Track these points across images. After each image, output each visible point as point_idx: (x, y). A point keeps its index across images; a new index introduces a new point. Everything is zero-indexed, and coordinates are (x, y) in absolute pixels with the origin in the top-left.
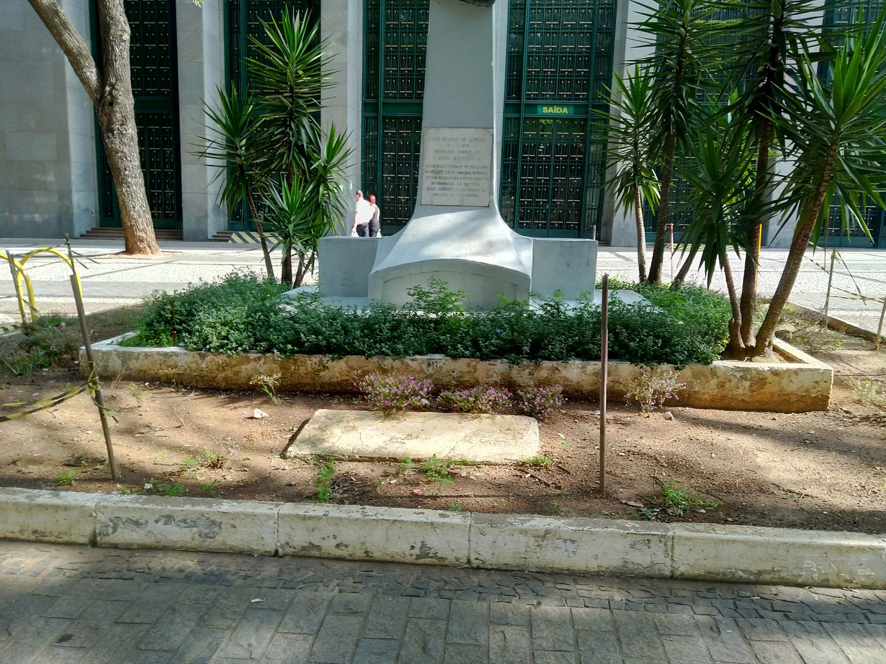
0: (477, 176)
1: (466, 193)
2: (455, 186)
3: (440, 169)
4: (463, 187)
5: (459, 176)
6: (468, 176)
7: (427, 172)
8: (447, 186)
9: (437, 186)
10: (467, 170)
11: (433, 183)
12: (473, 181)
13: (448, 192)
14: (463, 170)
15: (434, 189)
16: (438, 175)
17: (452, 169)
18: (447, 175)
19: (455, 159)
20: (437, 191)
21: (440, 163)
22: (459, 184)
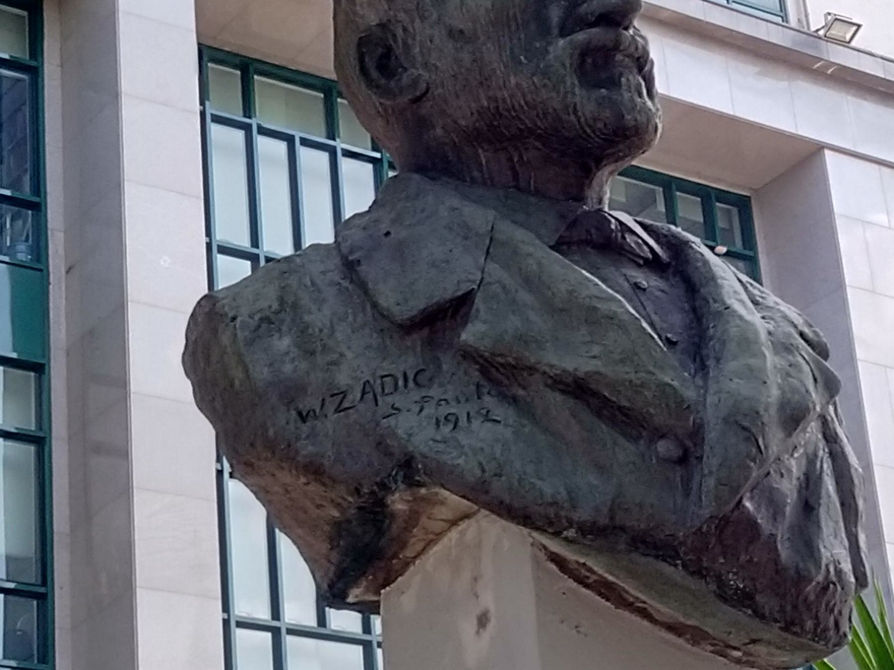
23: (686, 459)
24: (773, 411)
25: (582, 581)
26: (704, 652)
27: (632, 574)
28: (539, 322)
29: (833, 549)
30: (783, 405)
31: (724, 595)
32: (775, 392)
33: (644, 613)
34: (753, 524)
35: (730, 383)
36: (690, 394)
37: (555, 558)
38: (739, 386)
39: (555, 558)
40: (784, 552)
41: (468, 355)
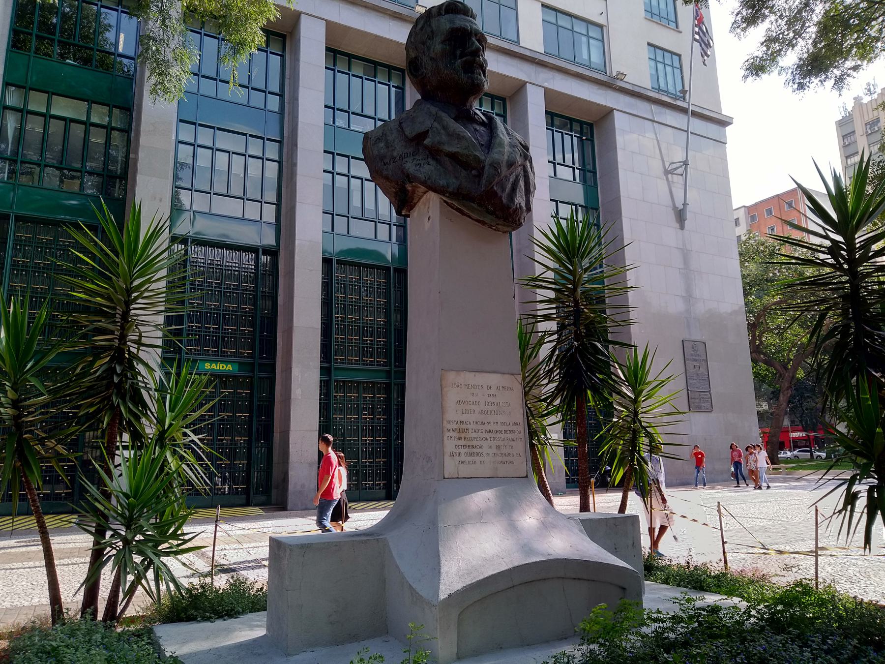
0: (509, 435)
1: (499, 459)
2: (485, 450)
3: (464, 426)
4: (495, 450)
5: (488, 435)
6: (498, 435)
7: (448, 430)
8: (475, 450)
9: (462, 451)
10: (498, 427)
11: (457, 447)
12: (506, 443)
13: (477, 459)
14: (493, 427)
15: (459, 454)
16: (463, 435)
17: (480, 427)
18: (474, 435)
19: (482, 412)
20: (463, 458)
21: (464, 418)
22: (489, 447)
23: (480, 175)
24: (504, 163)
25: (452, 208)
26: (486, 227)
27: (464, 206)
28: (444, 138)
29: (520, 200)
30: (508, 161)
31: (488, 212)
32: (506, 157)
33: (469, 217)
34: (495, 193)
35: (495, 155)
36: (483, 158)
37: (445, 202)
38: (496, 156)
39: (445, 202)
40: (504, 201)
41: (426, 147)
